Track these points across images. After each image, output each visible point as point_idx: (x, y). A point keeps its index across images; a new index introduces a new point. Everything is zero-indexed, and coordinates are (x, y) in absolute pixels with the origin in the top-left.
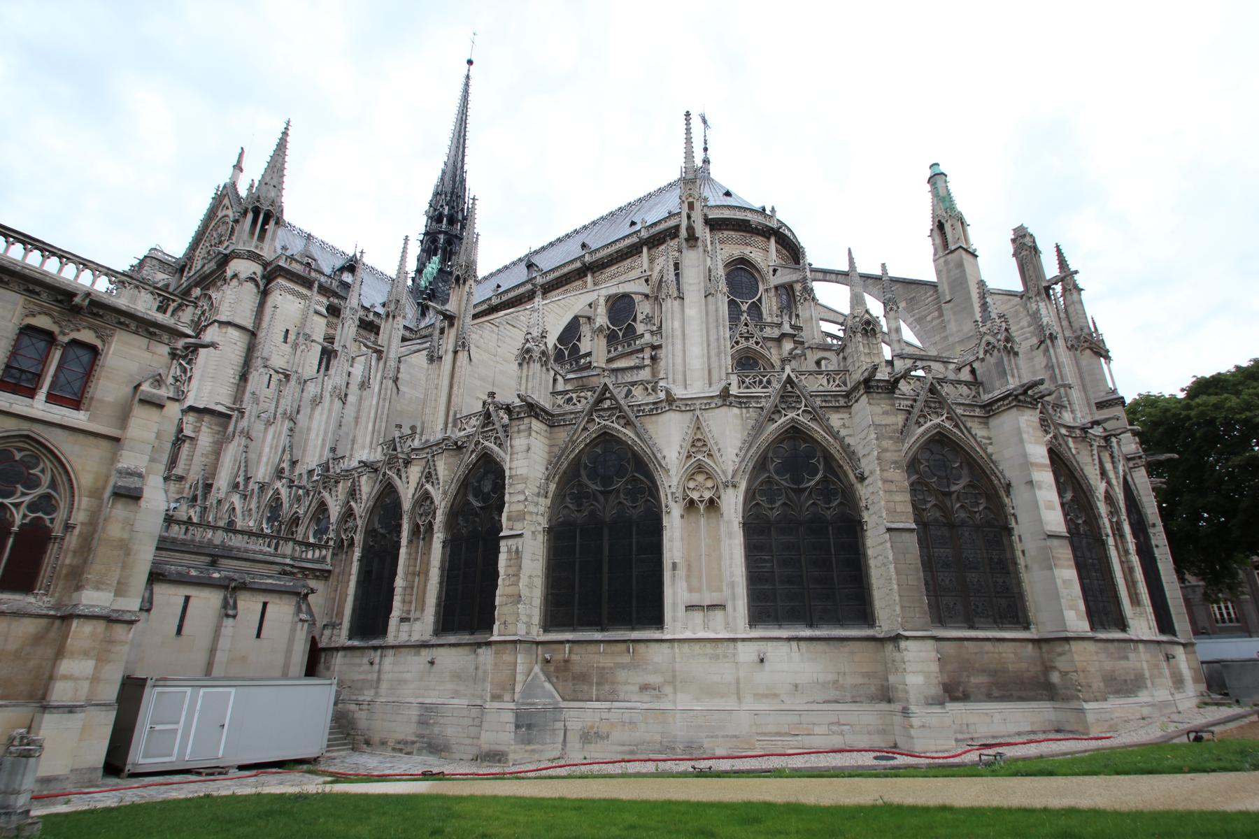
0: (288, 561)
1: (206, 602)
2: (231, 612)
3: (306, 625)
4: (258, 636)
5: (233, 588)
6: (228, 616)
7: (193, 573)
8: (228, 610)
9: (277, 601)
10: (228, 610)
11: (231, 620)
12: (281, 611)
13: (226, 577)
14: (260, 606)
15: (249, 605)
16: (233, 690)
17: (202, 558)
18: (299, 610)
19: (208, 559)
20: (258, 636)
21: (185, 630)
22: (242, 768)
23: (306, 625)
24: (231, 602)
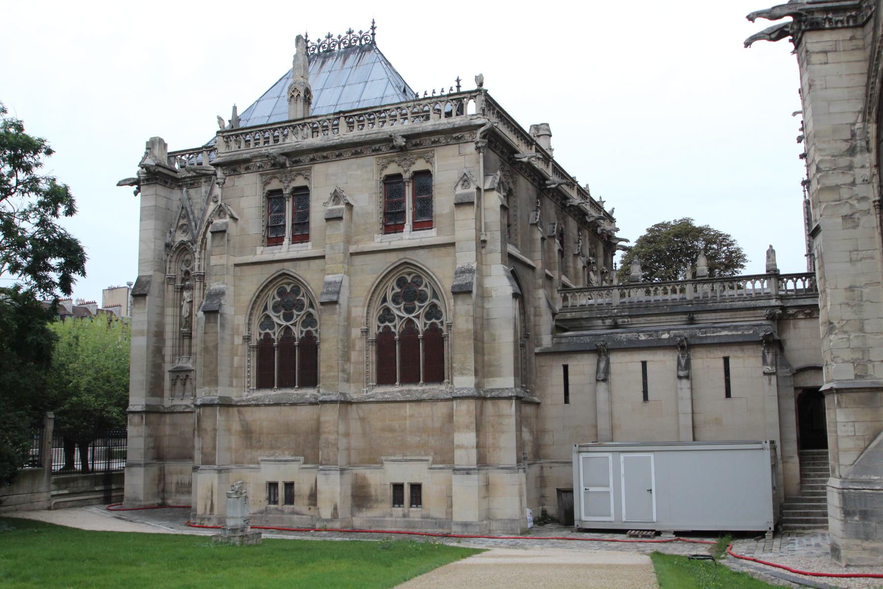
0: (773, 302)
1: (663, 364)
2: (682, 373)
3: (774, 378)
4: (728, 394)
5: (684, 347)
6: (680, 377)
7: (643, 337)
8: (685, 372)
9: (740, 354)
10: (685, 372)
11: (684, 381)
12: (748, 366)
13: (675, 336)
14: (721, 363)
15: (707, 364)
16: (652, 455)
17: (679, 317)
18: (765, 362)
19: (685, 317)
20: (728, 394)
21: (649, 398)
22: (678, 534)
23: (774, 378)
24: (683, 362)
